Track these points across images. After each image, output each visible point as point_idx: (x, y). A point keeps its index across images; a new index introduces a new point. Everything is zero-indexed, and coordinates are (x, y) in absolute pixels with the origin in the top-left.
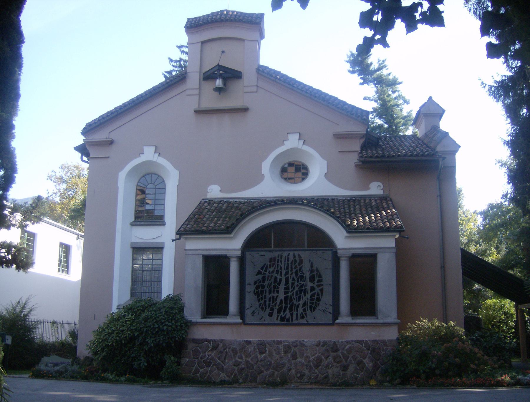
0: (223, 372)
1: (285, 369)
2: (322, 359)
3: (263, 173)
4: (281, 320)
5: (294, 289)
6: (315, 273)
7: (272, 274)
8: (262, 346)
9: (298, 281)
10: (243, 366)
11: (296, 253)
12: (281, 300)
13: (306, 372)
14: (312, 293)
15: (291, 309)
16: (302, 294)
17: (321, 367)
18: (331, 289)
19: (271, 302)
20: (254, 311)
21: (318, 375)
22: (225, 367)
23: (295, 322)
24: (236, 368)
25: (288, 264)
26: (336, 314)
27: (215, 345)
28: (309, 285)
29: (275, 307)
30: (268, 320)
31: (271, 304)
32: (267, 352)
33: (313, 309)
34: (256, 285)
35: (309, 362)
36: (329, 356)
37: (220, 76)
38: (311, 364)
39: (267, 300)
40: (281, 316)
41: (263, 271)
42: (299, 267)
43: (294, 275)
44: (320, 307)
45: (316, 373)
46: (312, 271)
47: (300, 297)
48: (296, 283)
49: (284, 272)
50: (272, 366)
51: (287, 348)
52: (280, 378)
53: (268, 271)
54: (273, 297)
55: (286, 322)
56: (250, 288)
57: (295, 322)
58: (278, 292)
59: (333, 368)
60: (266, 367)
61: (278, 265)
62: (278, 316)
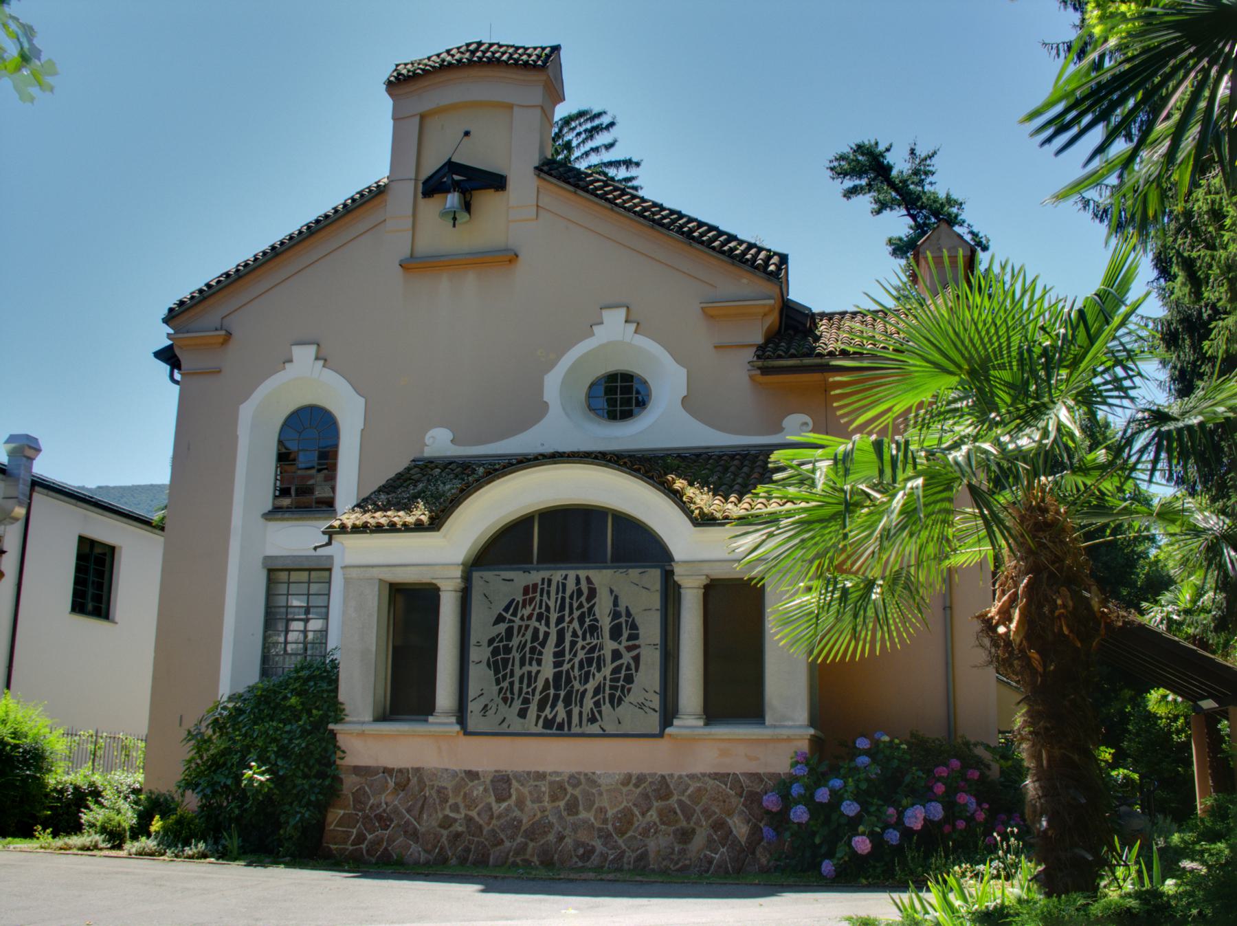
0: (417, 842)
1: (551, 837)
2: (633, 814)
3: (545, 399)
4: (545, 727)
5: (575, 655)
6: (623, 619)
7: (529, 623)
8: (502, 783)
9: (584, 639)
10: (460, 829)
11: (583, 574)
12: (547, 680)
13: (598, 844)
14: (615, 664)
15: (567, 702)
16: (593, 669)
17: (630, 834)
18: (657, 654)
19: (525, 686)
20: (486, 706)
21: (624, 852)
22: (422, 829)
23: (575, 730)
24: (445, 833)
25: (563, 599)
26: (669, 713)
27: (403, 779)
28: (610, 646)
29: (533, 695)
30: (517, 724)
31: (525, 690)
32: (514, 797)
33: (615, 702)
34: (492, 648)
35: (605, 821)
36: (648, 810)
37: (456, 186)
38: (610, 827)
39: (516, 679)
40: (546, 716)
41: (508, 616)
42: (586, 606)
43: (576, 624)
44: (631, 698)
45: (619, 847)
46: (616, 615)
47: (588, 674)
48: (580, 643)
49: (554, 617)
50: (523, 829)
51: (558, 790)
52: (538, 856)
53: (519, 615)
54: (530, 673)
55: (557, 729)
56: (479, 654)
57: (575, 730)
58: (539, 663)
59: (657, 838)
60: (509, 832)
61: (541, 601)
62: (538, 717)
